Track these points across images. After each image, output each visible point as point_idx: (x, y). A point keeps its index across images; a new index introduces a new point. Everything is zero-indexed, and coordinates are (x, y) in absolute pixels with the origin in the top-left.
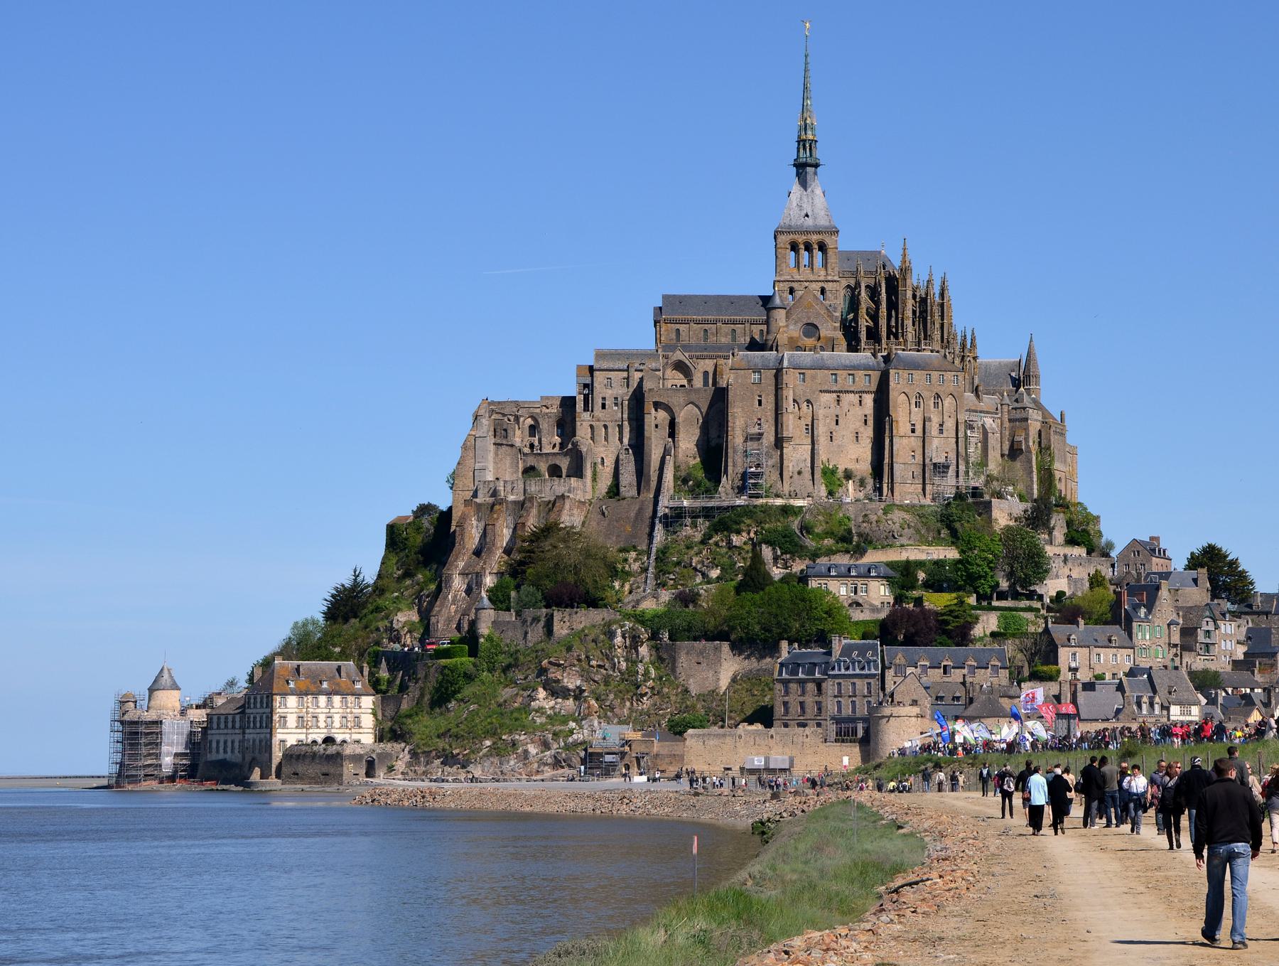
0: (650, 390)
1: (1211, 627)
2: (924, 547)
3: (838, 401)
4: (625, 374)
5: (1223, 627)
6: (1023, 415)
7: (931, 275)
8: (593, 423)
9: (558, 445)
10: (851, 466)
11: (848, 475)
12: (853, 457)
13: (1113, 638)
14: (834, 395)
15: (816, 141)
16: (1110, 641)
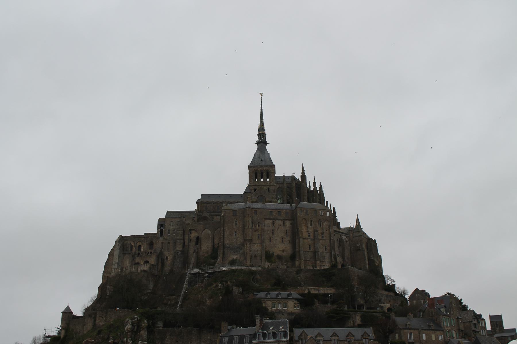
0: (189, 224)
1: (476, 322)
2: (317, 288)
3: (273, 223)
4: (179, 220)
5: (480, 322)
6: (360, 234)
7: (315, 180)
8: (164, 241)
9: (149, 253)
10: (280, 253)
11: (279, 257)
12: (281, 250)
13: (431, 325)
14: (271, 221)
15: (266, 135)
16: (430, 326)
